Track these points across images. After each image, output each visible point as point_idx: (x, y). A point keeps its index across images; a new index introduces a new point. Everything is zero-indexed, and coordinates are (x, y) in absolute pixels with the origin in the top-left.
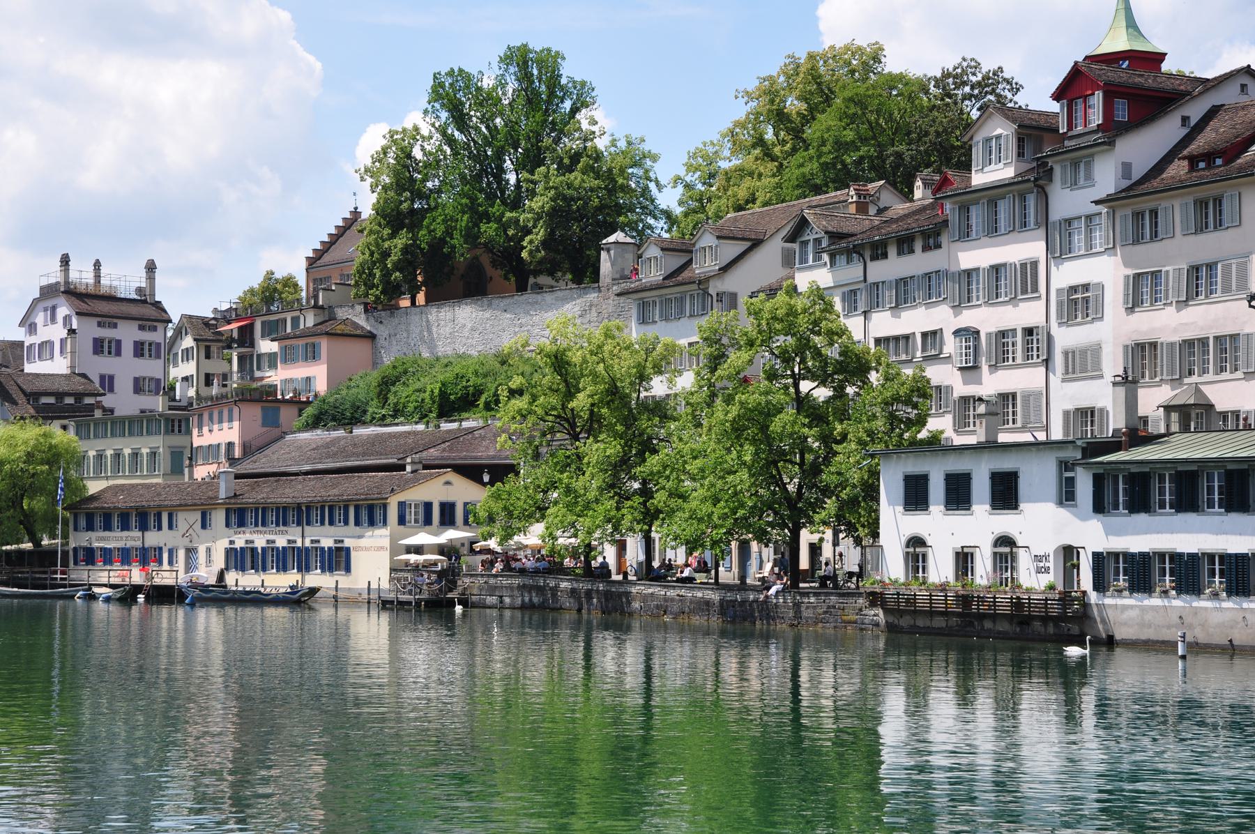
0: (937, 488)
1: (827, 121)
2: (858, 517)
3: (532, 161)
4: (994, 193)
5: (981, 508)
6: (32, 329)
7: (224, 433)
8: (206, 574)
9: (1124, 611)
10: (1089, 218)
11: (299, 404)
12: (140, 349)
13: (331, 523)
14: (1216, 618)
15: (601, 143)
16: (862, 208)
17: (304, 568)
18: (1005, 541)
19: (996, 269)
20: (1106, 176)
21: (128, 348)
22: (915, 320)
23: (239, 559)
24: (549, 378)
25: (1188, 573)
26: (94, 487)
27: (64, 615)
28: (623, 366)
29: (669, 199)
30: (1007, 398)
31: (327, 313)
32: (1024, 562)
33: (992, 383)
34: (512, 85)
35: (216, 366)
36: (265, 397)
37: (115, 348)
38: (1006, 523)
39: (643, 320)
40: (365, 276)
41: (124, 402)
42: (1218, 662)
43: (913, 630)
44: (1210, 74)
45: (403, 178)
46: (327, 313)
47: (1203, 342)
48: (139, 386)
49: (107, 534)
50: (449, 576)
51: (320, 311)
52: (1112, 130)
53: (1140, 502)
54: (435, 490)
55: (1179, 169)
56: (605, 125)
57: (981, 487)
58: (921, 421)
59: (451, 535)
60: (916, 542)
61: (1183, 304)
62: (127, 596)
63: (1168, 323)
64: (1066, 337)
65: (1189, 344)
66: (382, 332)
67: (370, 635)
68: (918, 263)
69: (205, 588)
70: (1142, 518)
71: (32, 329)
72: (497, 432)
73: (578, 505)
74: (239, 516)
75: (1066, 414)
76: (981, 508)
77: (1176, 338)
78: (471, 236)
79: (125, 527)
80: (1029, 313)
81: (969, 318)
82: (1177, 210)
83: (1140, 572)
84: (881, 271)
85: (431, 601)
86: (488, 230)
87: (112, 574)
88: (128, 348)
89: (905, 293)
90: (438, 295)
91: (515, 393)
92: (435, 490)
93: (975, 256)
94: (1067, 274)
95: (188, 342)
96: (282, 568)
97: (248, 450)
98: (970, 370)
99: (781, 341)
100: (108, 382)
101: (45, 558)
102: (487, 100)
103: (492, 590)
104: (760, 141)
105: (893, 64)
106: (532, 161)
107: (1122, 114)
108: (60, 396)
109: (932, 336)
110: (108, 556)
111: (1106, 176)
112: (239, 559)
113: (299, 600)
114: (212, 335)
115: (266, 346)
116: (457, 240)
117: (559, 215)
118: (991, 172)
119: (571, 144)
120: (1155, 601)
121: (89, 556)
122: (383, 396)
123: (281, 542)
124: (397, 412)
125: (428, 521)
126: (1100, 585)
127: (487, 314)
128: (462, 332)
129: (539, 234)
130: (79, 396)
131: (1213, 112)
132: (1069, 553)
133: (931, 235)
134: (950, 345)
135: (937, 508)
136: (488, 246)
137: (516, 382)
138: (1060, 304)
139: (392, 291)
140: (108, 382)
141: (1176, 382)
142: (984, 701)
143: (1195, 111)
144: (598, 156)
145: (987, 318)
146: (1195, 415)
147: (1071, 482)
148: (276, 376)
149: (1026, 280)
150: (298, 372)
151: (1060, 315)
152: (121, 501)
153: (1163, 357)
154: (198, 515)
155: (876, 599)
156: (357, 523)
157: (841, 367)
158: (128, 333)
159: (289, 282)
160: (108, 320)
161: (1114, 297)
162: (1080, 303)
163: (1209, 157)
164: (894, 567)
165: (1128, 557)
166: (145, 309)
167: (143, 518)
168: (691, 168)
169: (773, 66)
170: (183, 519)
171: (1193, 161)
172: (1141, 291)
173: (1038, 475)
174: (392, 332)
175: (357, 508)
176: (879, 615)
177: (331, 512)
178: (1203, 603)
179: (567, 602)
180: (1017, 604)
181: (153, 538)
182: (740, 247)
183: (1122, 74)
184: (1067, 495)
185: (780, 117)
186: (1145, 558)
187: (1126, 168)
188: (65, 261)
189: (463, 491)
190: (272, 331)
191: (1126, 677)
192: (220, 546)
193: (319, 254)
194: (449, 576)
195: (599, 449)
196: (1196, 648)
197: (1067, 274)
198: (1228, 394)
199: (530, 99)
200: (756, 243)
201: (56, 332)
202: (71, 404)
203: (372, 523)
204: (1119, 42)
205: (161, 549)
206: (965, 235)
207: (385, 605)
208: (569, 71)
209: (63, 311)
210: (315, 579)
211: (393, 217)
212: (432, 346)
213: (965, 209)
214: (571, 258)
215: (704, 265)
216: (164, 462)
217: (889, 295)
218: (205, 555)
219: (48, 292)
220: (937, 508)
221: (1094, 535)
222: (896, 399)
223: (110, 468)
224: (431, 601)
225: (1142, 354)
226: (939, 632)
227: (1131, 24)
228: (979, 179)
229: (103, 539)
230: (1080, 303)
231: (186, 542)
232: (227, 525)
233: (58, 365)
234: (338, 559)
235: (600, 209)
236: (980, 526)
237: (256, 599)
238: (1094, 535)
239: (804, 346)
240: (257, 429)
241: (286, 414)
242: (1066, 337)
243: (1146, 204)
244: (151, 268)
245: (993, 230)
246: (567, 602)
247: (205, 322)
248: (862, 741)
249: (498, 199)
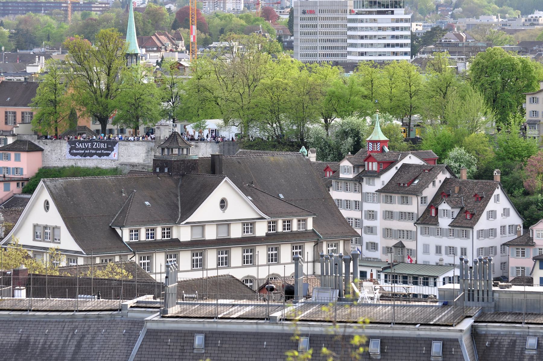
4: (347, 180)
10: (374, 194)
47: (403, 231)
51: (14, 137)
75: (367, 243)
77: (396, 229)
94: (367, 206)
138: (365, 215)
147: (379, 275)
151: (365, 218)
187: (383, 182)
197: (367, 206)
225: (388, 233)
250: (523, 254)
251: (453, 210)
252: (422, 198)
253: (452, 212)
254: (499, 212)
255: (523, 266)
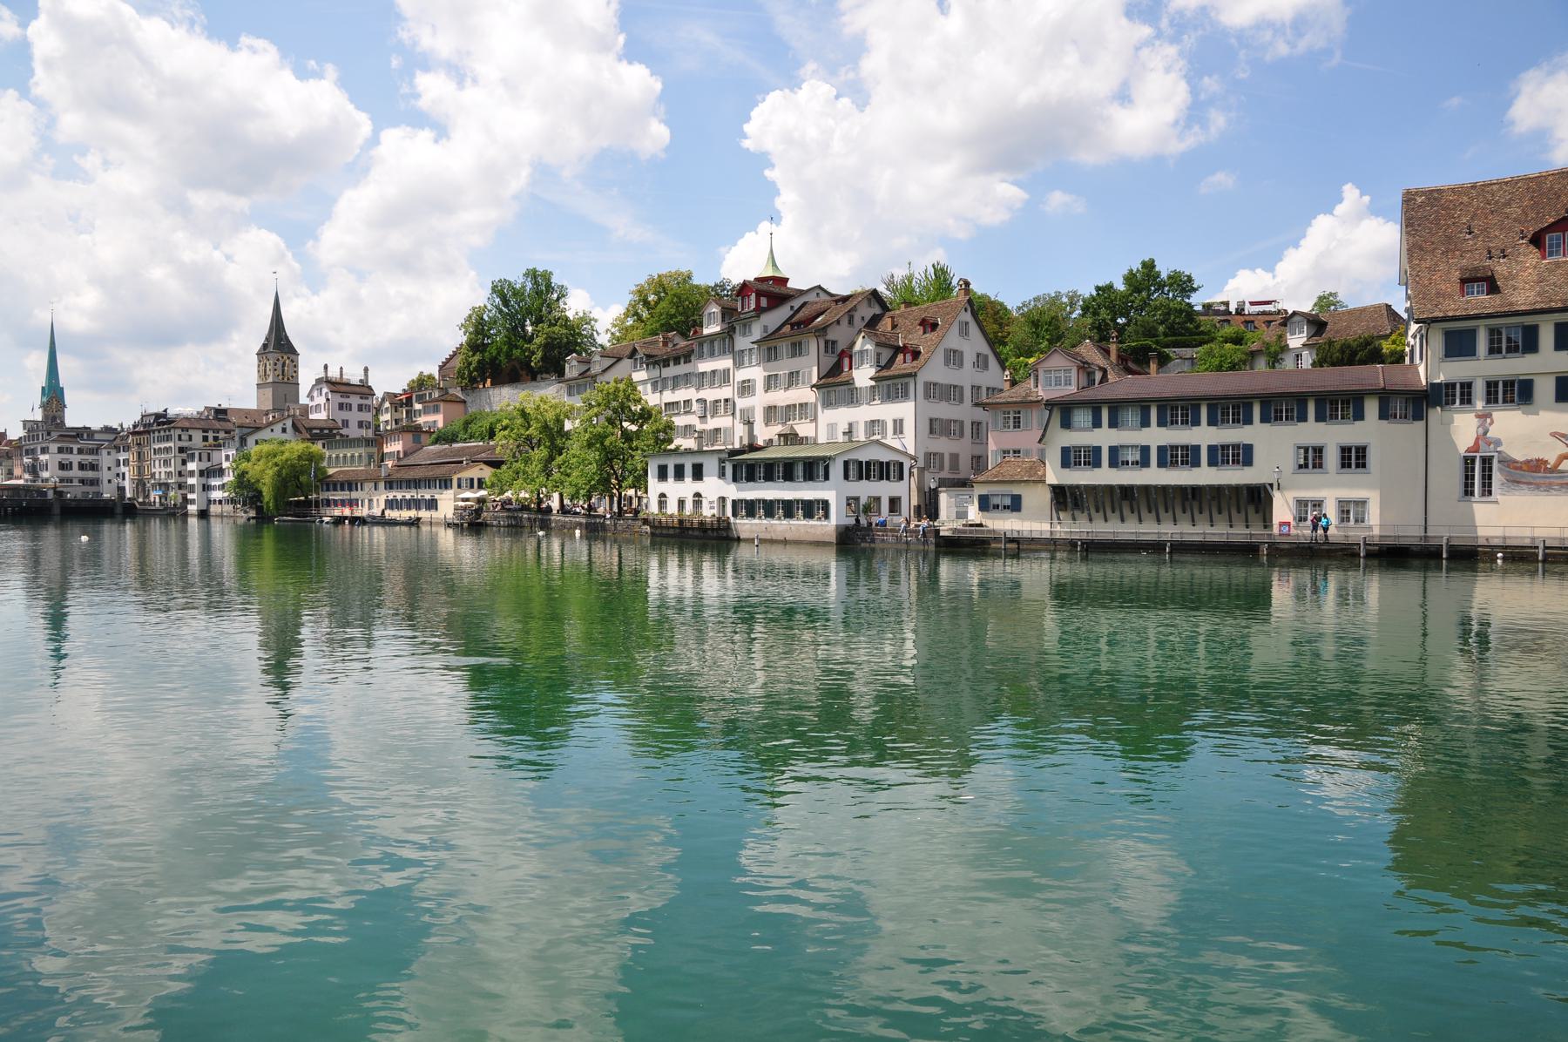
0: (671, 471)
1: (663, 304)
2: (640, 482)
3: (539, 320)
5: (688, 479)
6: (312, 399)
7: (394, 447)
8: (377, 512)
9: (745, 526)
11: (429, 433)
12: (360, 408)
14: (779, 528)
15: (570, 314)
16: (665, 344)
17: (418, 508)
18: (698, 495)
19: (714, 372)
20: (757, 332)
21: (355, 407)
22: (681, 395)
23: (391, 504)
24: (519, 421)
25: (769, 508)
26: (331, 471)
27: (317, 532)
28: (550, 416)
29: (603, 339)
30: (717, 430)
31: (444, 391)
32: (705, 504)
33: (712, 423)
34: (529, 285)
35: (397, 416)
36: (416, 431)
37: (349, 407)
38: (698, 486)
39: (570, 394)
40: (460, 375)
41: (353, 432)
42: (781, 547)
43: (661, 535)
44: (805, 288)
45: (479, 327)
46: (444, 391)
48: (360, 424)
50: (478, 512)
52: (759, 311)
53: (751, 478)
54: (476, 472)
55: (787, 329)
56: (575, 305)
57: (688, 470)
58: (670, 441)
59: (483, 493)
60: (663, 495)
61: (787, 389)
62: (339, 521)
63: (781, 397)
64: (741, 403)
65: (788, 406)
66: (469, 399)
67: (447, 538)
68: (682, 369)
69: (374, 517)
70: (751, 484)
71: (312, 399)
72: (502, 445)
73: (529, 480)
74: (390, 485)
76: (688, 479)
78: (509, 356)
79: (342, 489)
80: (725, 392)
81: (703, 394)
82: (784, 347)
83: (750, 508)
84: (671, 371)
85: (472, 524)
86: (516, 352)
88: (355, 407)
89: (676, 382)
90: (498, 381)
91: (505, 428)
92: (476, 472)
93: (705, 366)
94: (741, 375)
95: (387, 405)
96: (409, 508)
97: (406, 454)
98: (703, 418)
99: (614, 404)
100: (346, 423)
101: (307, 504)
102: (516, 293)
103: (496, 518)
104: (636, 314)
105: (696, 281)
106: (538, 321)
107: (764, 302)
108: (322, 429)
109: (688, 402)
110: (336, 503)
111: (757, 332)
112: (391, 504)
113: (415, 523)
114: (402, 402)
115: (418, 406)
116: (502, 358)
117: (548, 347)
118: (712, 328)
119: (556, 314)
120: (756, 521)
121: (328, 503)
122: (465, 429)
123: (408, 496)
124: (471, 437)
125: (472, 486)
126: (735, 514)
128: (504, 399)
129: (539, 354)
130: (331, 430)
131: (805, 304)
132: (723, 499)
133: (687, 357)
134: (695, 406)
135: (671, 480)
136: (517, 359)
137: (505, 422)
139: (473, 380)
140: (346, 423)
141: (784, 424)
142: (689, 564)
143: (797, 303)
144: (567, 319)
145: (710, 394)
146: (790, 438)
148: (421, 420)
149: (725, 377)
150: (430, 418)
152: (341, 478)
153: (779, 414)
155: (646, 521)
157: (641, 416)
158: (355, 401)
159: (431, 377)
160: (345, 394)
161: (760, 385)
162: (746, 388)
163: (798, 324)
164: (654, 508)
165: (746, 501)
166: (364, 390)
167: (350, 485)
168: (614, 326)
169: (642, 280)
171: (792, 325)
172: (771, 383)
173: (710, 465)
176: (647, 528)
177: (428, 483)
178: (775, 522)
179: (526, 523)
180: (701, 523)
181: (354, 495)
182: (611, 361)
183: (764, 287)
184: (722, 475)
185: (646, 303)
186: (752, 501)
187: (766, 328)
188: (326, 367)
189: (487, 473)
190: (420, 399)
191: (744, 553)
192: (383, 498)
193: (445, 364)
194: (478, 512)
195: (540, 453)
196: (762, 541)
197: (741, 375)
198: (804, 429)
199: (539, 293)
200: (619, 359)
201: (321, 400)
202: (327, 434)
204: (769, 273)
206: (701, 357)
207: (449, 525)
208: (555, 280)
209: (325, 390)
210: (424, 514)
211: (474, 346)
212: (490, 405)
213: (701, 345)
214: (552, 366)
215: (596, 369)
216: (365, 460)
217: (670, 383)
218: (375, 502)
219: (319, 381)
220: (671, 480)
221: (733, 492)
222: (658, 431)
223: (337, 461)
224: (472, 524)
225: (771, 412)
226: (668, 536)
227: (774, 264)
228: (706, 331)
230: (746, 388)
233: (322, 416)
234: (432, 504)
235: (568, 343)
236: (688, 488)
237: (394, 523)
238: (733, 492)
239: (623, 406)
240: (410, 444)
241: (424, 438)
242: (741, 403)
243: (772, 344)
244: (366, 370)
245: (712, 354)
246: (526, 523)
247: (395, 395)
248: (641, 581)
249: (519, 339)
250: (1017, 424)
251: (880, 350)
252: (827, 342)
253: (878, 355)
254: (969, 358)
255: (1016, 447)
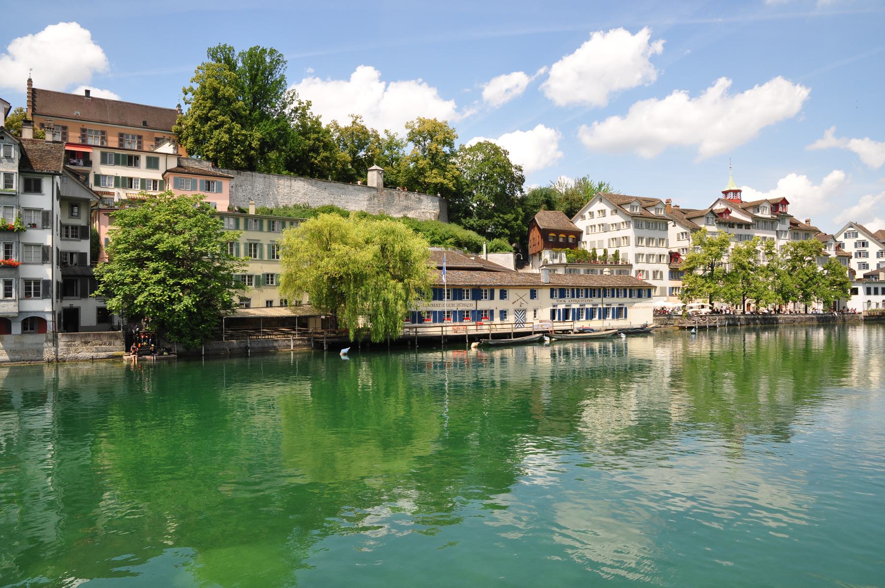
0: (872, 291)
13: (618, 296)
49: (437, 302)
74: (559, 291)
87: (444, 329)
110: (440, 317)
127: (315, 188)
154: (528, 292)
156: (631, 296)
170: (512, 294)
174: (238, 183)
175: (631, 291)
181: (483, 304)
203: (640, 296)
205: (492, 312)
229: (433, 305)
231: (517, 306)
232: (552, 297)
